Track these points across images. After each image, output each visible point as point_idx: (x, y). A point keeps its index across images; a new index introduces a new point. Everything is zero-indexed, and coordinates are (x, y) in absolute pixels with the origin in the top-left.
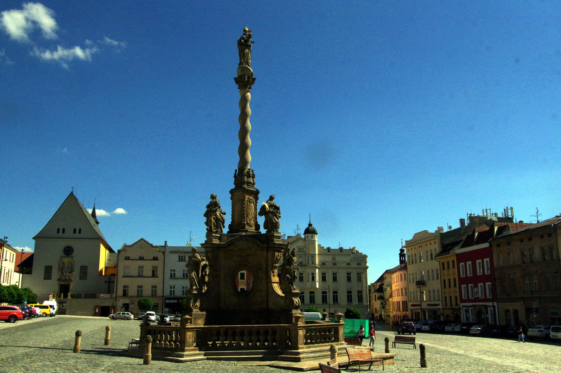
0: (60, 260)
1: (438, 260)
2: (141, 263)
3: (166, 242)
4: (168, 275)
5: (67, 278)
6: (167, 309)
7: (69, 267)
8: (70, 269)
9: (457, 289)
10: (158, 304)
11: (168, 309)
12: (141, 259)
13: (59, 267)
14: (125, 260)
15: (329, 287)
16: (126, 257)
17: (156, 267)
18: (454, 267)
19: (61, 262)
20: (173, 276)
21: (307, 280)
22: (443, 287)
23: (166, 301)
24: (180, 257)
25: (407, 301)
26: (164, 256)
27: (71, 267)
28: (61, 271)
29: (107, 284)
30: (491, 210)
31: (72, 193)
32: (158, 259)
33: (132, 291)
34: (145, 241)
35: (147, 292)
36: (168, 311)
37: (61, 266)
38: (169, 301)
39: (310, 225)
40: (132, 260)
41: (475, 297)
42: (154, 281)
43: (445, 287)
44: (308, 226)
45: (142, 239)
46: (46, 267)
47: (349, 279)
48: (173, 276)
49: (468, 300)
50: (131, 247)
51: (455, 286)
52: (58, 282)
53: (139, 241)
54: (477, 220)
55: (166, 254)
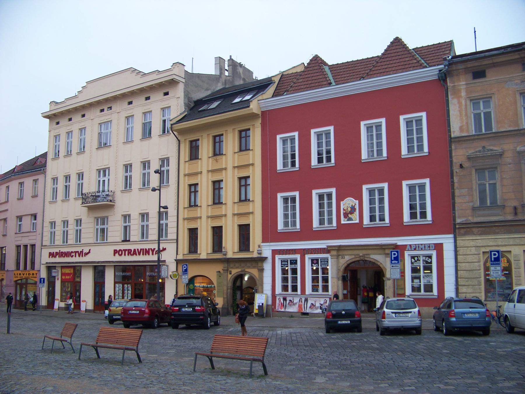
25: (33, 246)
43: (193, 205)
51: (244, 200)
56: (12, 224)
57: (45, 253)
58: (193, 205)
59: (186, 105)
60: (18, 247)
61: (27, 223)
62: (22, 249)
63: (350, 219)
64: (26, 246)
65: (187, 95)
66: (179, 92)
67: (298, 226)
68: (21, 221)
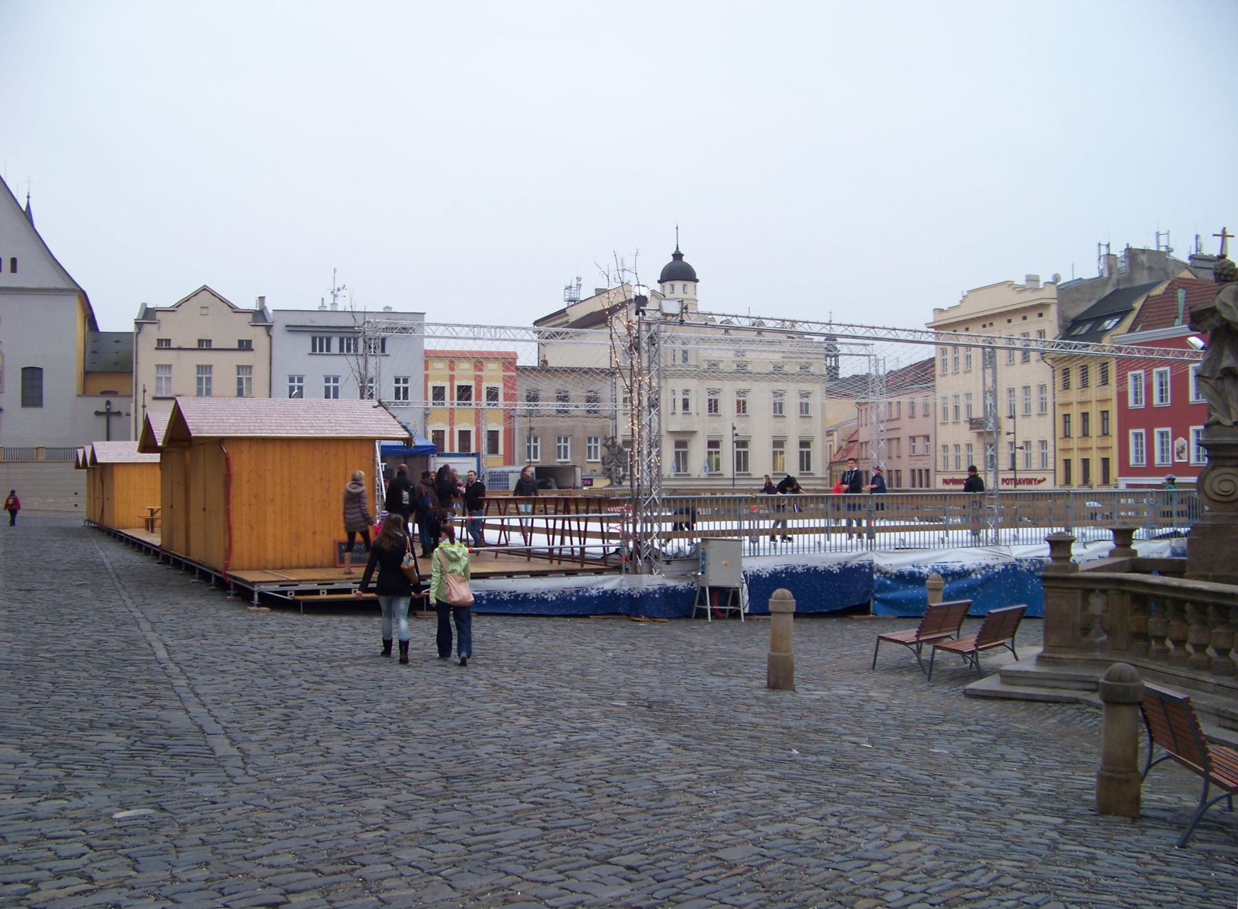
1: (1049, 361)
2: (204, 358)
3: (262, 299)
9: (1113, 441)
12: (204, 345)
15: (734, 428)
16: (160, 341)
18: (1105, 381)
21: (670, 411)
22: (1060, 433)
24: (314, 339)
25: (927, 471)
26: (271, 337)
30: (1171, 234)
32: (253, 346)
34: (214, 294)
39: (678, 256)
40: (179, 349)
41: (1174, 463)
43: (1067, 436)
44: (671, 259)
45: (205, 289)
47: (778, 409)
49: (1150, 470)
51: (1105, 434)
53: (196, 294)
54: (1143, 258)
55: (274, 333)
56: (905, 443)
57: (939, 479)
58: (1067, 436)
59: (1060, 326)
60: (913, 471)
61: (919, 443)
62: (917, 473)
63: (1181, 458)
64: (920, 471)
65: (1061, 315)
66: (1052, 315)
67: (1144, 463)
68: (914, 441)
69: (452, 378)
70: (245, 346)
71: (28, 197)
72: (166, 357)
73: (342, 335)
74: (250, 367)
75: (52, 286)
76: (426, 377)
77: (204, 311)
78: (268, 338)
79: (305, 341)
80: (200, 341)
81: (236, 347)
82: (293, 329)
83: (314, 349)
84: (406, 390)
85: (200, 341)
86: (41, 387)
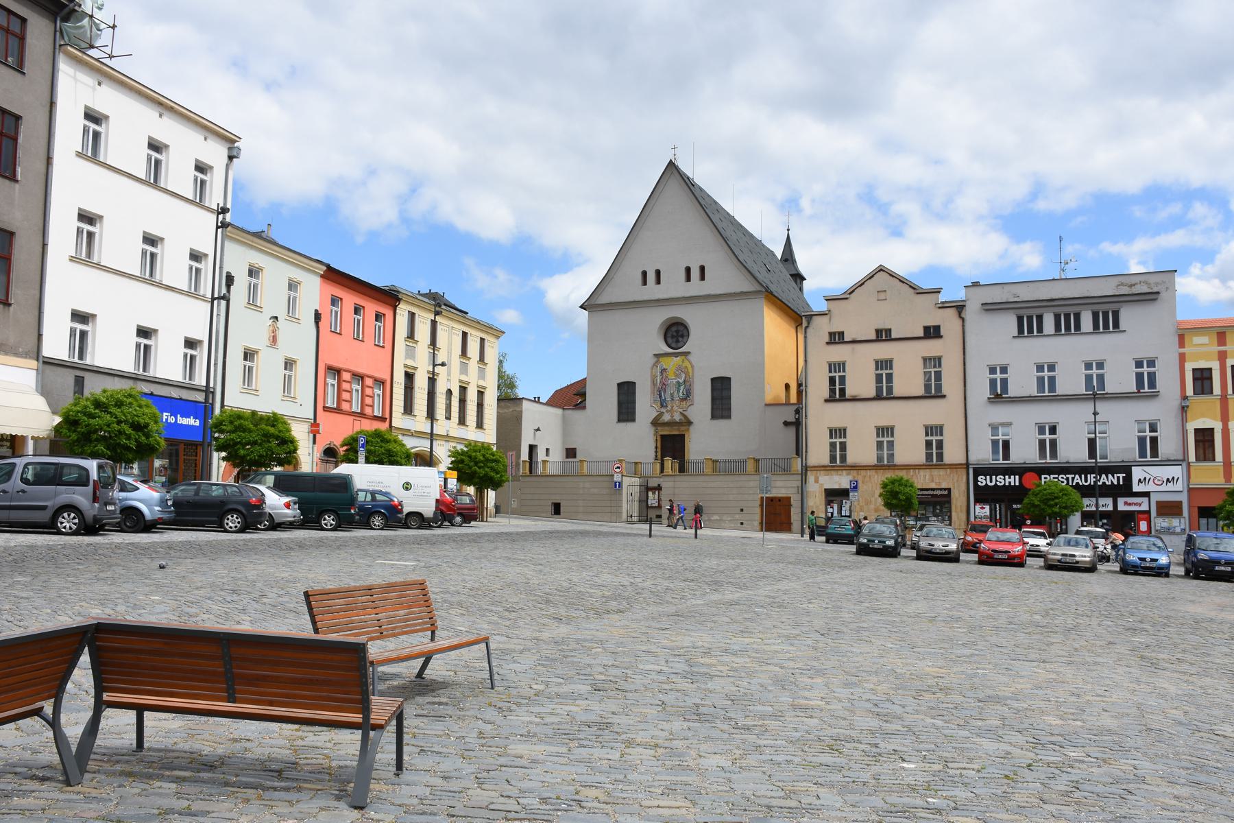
0: (655, 365)
2: (883, 350)
4: (980, 389)
5: (677, 417)
6: (982, 508)
7: (679, 384)
8: (682, 388)
10: (949, 490)
11: (987, 507)
12: (883, 335)
13: (654, 384)
14: (827, 343)
16: (832, 335)
17: (938, 361)
19: (659, 370)
20: (999, 395)
23: (979, 478)
24: (1020, 319)
26: (963, 320)
27: (685, 381)
28: (660, 397)
29: (792, 430)
31: (671, 165)
33: (862, 450)
34: (892, 275)
35: (909, 449)
36: (988, 514)
37: (658, 382)
38: (991, 481)
40: (854, 342)
42: (932, 412)
45: (881, 269)
46: (620, 385)
48: (999, 395)
50: (847, 298)
52: (652, 430)
53: (871, 277)
55: (968, 314)
69: (1222, 357)
70: (932, 333)
71: (788, 230)
72: (838, 353)
73: (1058, 310)
74: (940, 359)
75: (738, 290)
76: (1182, 358)
77: (882, 296)
78: (959, 322)
79: (1009, 322)
80: (878, 332)
81: (922, 335)
82: (990, 308)
83: (1021, 331)
84: (1152, 377)
85: (878, 332)
86: (729, 398)
